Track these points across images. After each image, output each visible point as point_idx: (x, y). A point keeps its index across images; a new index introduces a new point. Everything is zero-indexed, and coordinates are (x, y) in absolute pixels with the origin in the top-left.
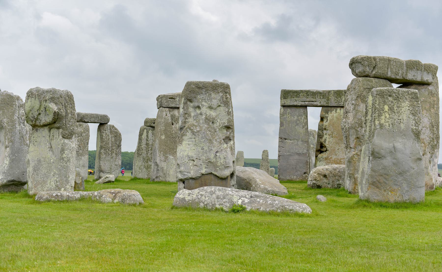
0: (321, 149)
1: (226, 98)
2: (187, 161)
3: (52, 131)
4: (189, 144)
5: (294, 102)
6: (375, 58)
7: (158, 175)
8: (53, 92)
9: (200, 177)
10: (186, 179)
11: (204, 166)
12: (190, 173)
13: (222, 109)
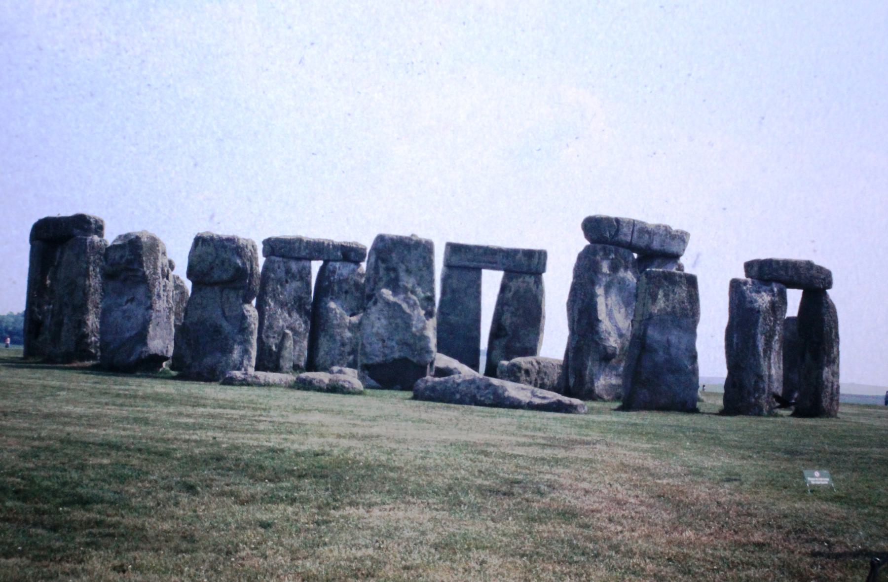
3: (226, 292)
4: (379, 319)
10: (372, 365)
11: (396, 348)
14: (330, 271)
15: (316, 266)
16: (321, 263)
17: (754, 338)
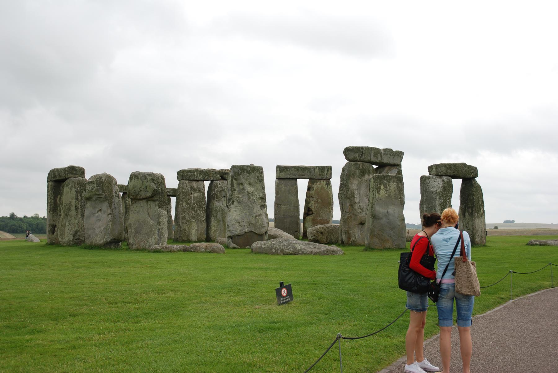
0: (308, 212)
3: (149, 203)
5: (287, 175)
6: (362, 148)
8: (151, 175)
11: (246, 226)
13: (258, 185)
14: (214, 186)
15: (207, 184)
16: (209, 182)
17: (434, 206)
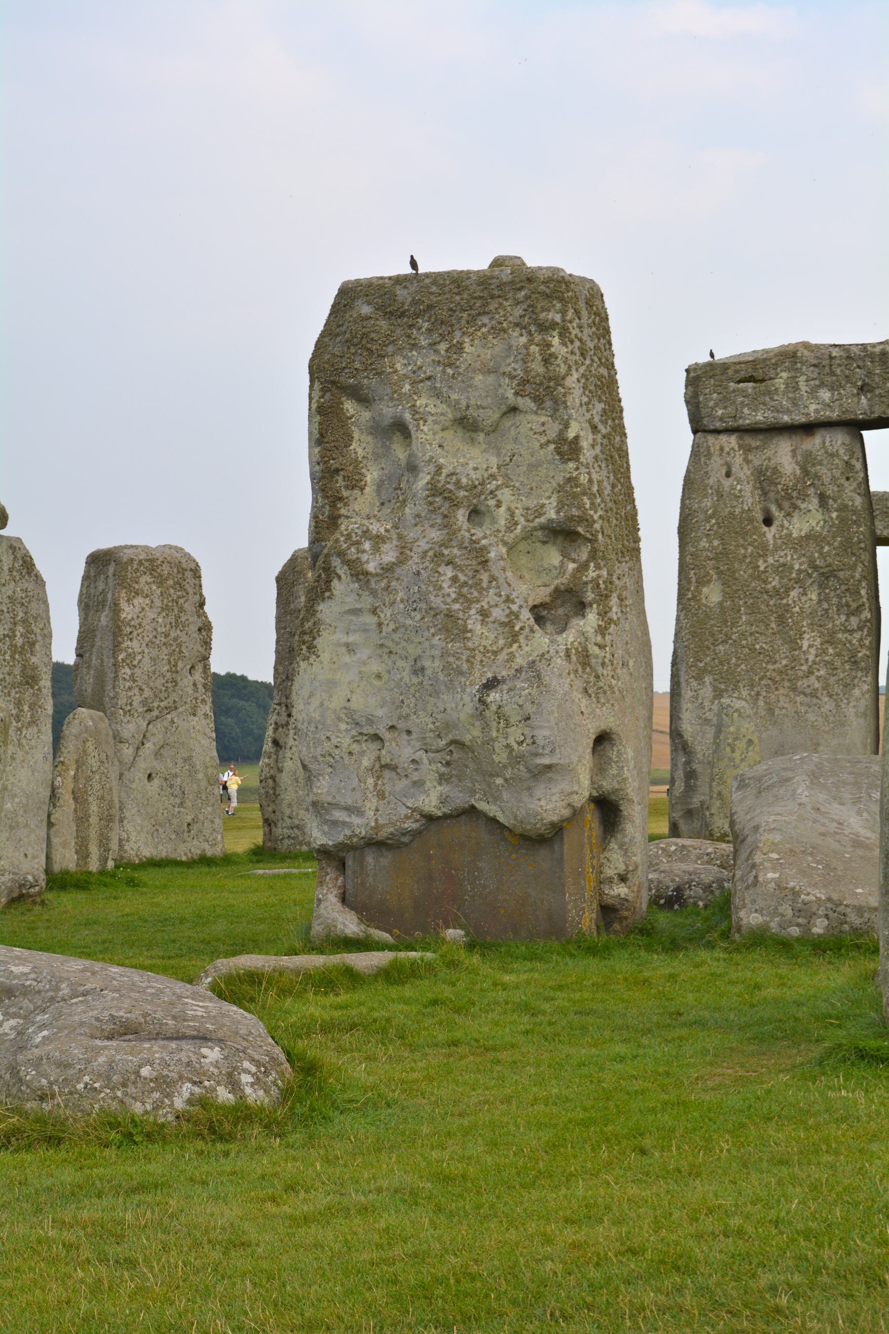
1: (547, 360)
2: (346, 741)
4: (350, 648)
7: (696, 801)
9: (416, 834)
10: (343, 847)
11: (430, 770)
12: (359, 812)
